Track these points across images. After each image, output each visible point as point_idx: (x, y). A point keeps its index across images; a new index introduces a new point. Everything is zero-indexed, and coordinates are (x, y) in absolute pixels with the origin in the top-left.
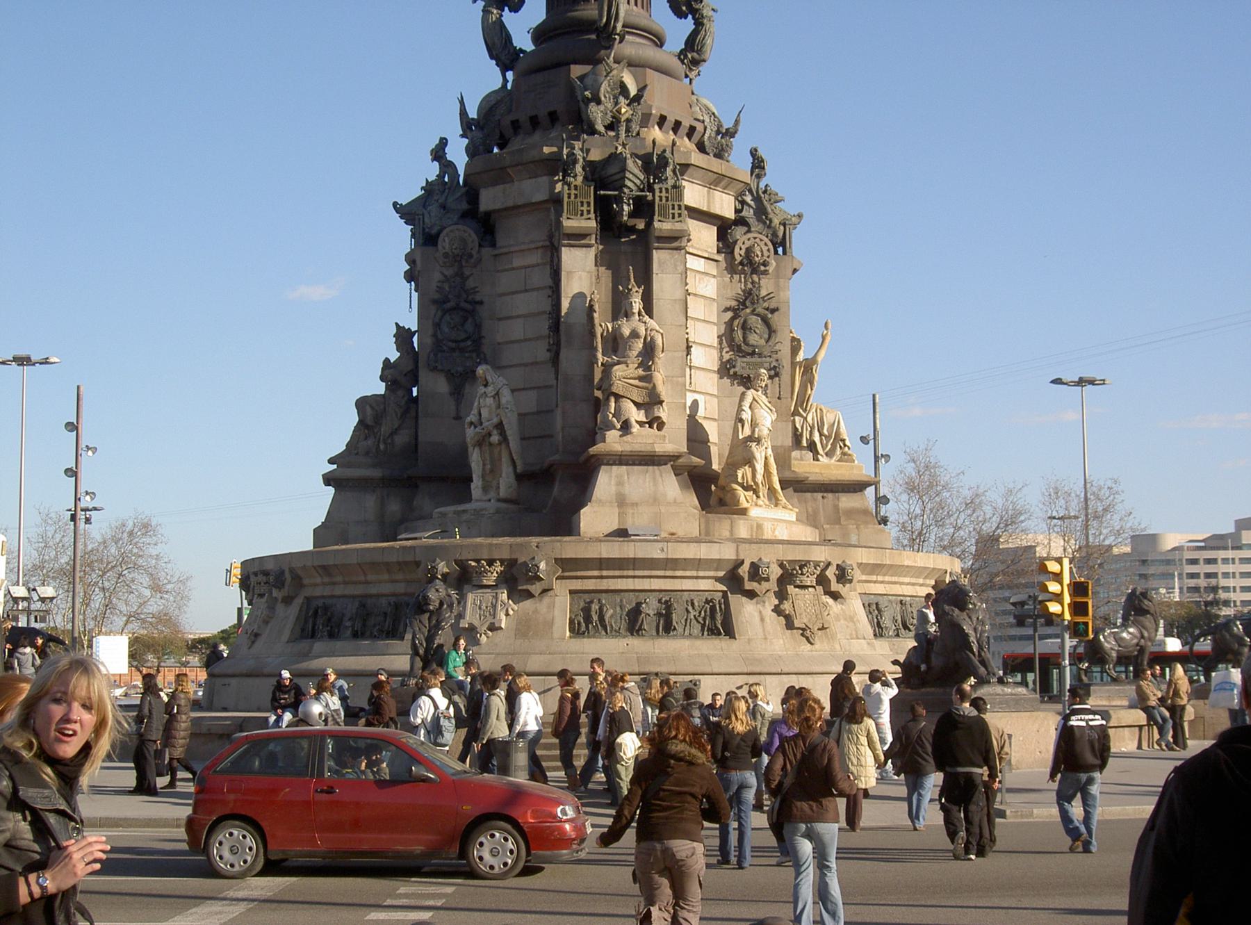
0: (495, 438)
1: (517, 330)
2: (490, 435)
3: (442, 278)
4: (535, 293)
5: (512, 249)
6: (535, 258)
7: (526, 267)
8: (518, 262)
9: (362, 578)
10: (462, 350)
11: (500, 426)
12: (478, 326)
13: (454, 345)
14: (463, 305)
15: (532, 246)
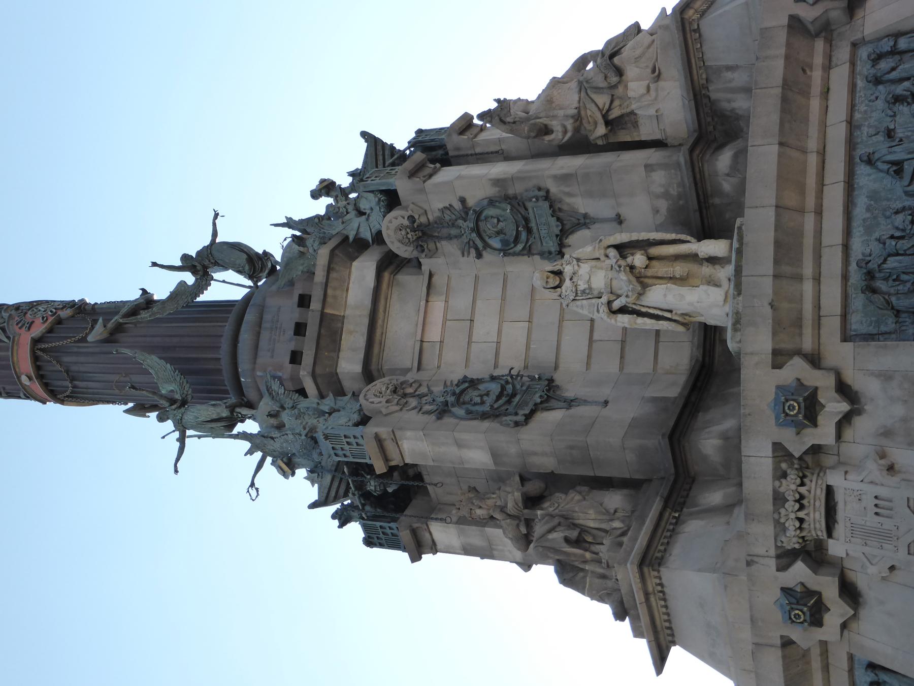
0: (639, 259)
1: (515, 334)
2: (632, 268)
3: (417, 410)
4: (479, 303)
5: (419, 338)
6: (438, 305)
7: (445, 320)
8: (434, 335)
9: (813, 160)
10: (514, 395)
11: (622, 249)
12: (493, 378)
13: (504, 399)
14: (457, 392)
15: (423, 303)
